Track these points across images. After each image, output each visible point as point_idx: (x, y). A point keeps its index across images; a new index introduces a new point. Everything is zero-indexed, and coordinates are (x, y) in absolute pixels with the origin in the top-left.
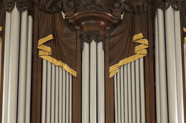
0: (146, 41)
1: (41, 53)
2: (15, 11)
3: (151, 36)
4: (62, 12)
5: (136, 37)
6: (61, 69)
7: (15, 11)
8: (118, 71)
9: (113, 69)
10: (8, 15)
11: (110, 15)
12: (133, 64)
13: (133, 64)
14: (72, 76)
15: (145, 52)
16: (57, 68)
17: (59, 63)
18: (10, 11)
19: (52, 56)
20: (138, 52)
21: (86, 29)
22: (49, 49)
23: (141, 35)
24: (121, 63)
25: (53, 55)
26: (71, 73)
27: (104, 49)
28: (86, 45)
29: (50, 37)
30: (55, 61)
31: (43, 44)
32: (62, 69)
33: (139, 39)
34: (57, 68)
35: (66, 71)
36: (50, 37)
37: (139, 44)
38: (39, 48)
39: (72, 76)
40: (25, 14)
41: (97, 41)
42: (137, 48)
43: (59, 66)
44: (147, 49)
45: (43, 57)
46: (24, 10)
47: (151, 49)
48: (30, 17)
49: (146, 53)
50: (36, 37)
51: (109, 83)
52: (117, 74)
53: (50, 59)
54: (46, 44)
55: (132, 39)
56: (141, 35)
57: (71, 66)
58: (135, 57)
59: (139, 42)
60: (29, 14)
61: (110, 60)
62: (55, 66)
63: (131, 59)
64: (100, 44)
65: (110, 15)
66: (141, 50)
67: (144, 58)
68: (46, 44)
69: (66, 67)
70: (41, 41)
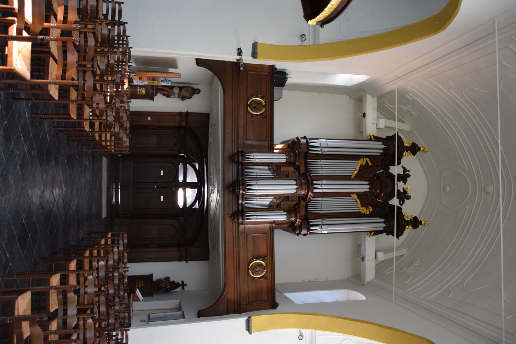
0: (368, 213)
1: (362, 159)
2: (383, 146)
3: (371, 215)
4: (383, 170)
5: (370, 208)
6: (354, 170)
7: (383, 146)
8: (354, 199)
9: (355, 196)
10: (381, 143)
11: (383, 195)
12: (357, 206)
13: (357, 206)
14: (351, 176)
15: (363, 212)
16: (355, 168)
17: (357, 169)
18: (383, 144)
19: (361, 166)
20: (363, 209)
21: (375, 182)
22: (364, 163)
23: (371, 210)
24: (358, 200)
25: (361, 166)
26: (353, 175)
27: (365, 192)
28: (367, 183)
29: (370, 164)
30: (358, 167)
31: (367, 161)
32: (354, 170)
33: (369, 210)
34: (355, 168)
35: (354, 172)
36: (370, 164)
37: (367, 210)
38: (365, 158)
39: (351, 176)
40: (381, 151)
41: (369, 188)
42: (365, 208)
43: (356, 169)
44: (364, 213)
45: (360, 160)
46: (384, 151)
47: (364, 216)
48: (380, 154)
49: (362, 213)
50: (371, 157)
51: (348, 194)
52: (352, 198)
53: (359, 164)
54: (367, 162)
55: (370, 206)
56: (371, 210)
57: (356, 175)
58: (360, 208)
59: (368, 210)
60: (381, 153)
61: (359, 195)
62: (356, 167)
63: (360, 205)
64: (368, 190)
65: (383, 195)
66: (364, 211)
67: (360, 212)
68: (367, 162)
69: (356, 172)
70: (368, 160)
